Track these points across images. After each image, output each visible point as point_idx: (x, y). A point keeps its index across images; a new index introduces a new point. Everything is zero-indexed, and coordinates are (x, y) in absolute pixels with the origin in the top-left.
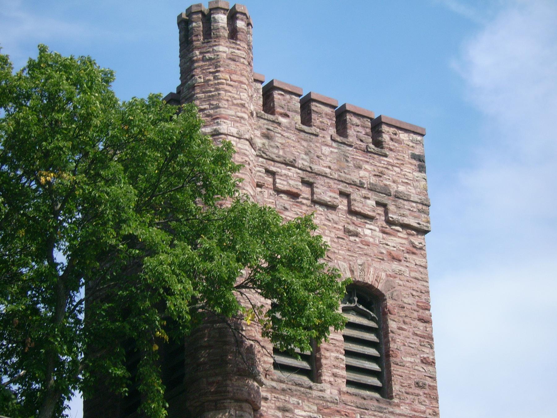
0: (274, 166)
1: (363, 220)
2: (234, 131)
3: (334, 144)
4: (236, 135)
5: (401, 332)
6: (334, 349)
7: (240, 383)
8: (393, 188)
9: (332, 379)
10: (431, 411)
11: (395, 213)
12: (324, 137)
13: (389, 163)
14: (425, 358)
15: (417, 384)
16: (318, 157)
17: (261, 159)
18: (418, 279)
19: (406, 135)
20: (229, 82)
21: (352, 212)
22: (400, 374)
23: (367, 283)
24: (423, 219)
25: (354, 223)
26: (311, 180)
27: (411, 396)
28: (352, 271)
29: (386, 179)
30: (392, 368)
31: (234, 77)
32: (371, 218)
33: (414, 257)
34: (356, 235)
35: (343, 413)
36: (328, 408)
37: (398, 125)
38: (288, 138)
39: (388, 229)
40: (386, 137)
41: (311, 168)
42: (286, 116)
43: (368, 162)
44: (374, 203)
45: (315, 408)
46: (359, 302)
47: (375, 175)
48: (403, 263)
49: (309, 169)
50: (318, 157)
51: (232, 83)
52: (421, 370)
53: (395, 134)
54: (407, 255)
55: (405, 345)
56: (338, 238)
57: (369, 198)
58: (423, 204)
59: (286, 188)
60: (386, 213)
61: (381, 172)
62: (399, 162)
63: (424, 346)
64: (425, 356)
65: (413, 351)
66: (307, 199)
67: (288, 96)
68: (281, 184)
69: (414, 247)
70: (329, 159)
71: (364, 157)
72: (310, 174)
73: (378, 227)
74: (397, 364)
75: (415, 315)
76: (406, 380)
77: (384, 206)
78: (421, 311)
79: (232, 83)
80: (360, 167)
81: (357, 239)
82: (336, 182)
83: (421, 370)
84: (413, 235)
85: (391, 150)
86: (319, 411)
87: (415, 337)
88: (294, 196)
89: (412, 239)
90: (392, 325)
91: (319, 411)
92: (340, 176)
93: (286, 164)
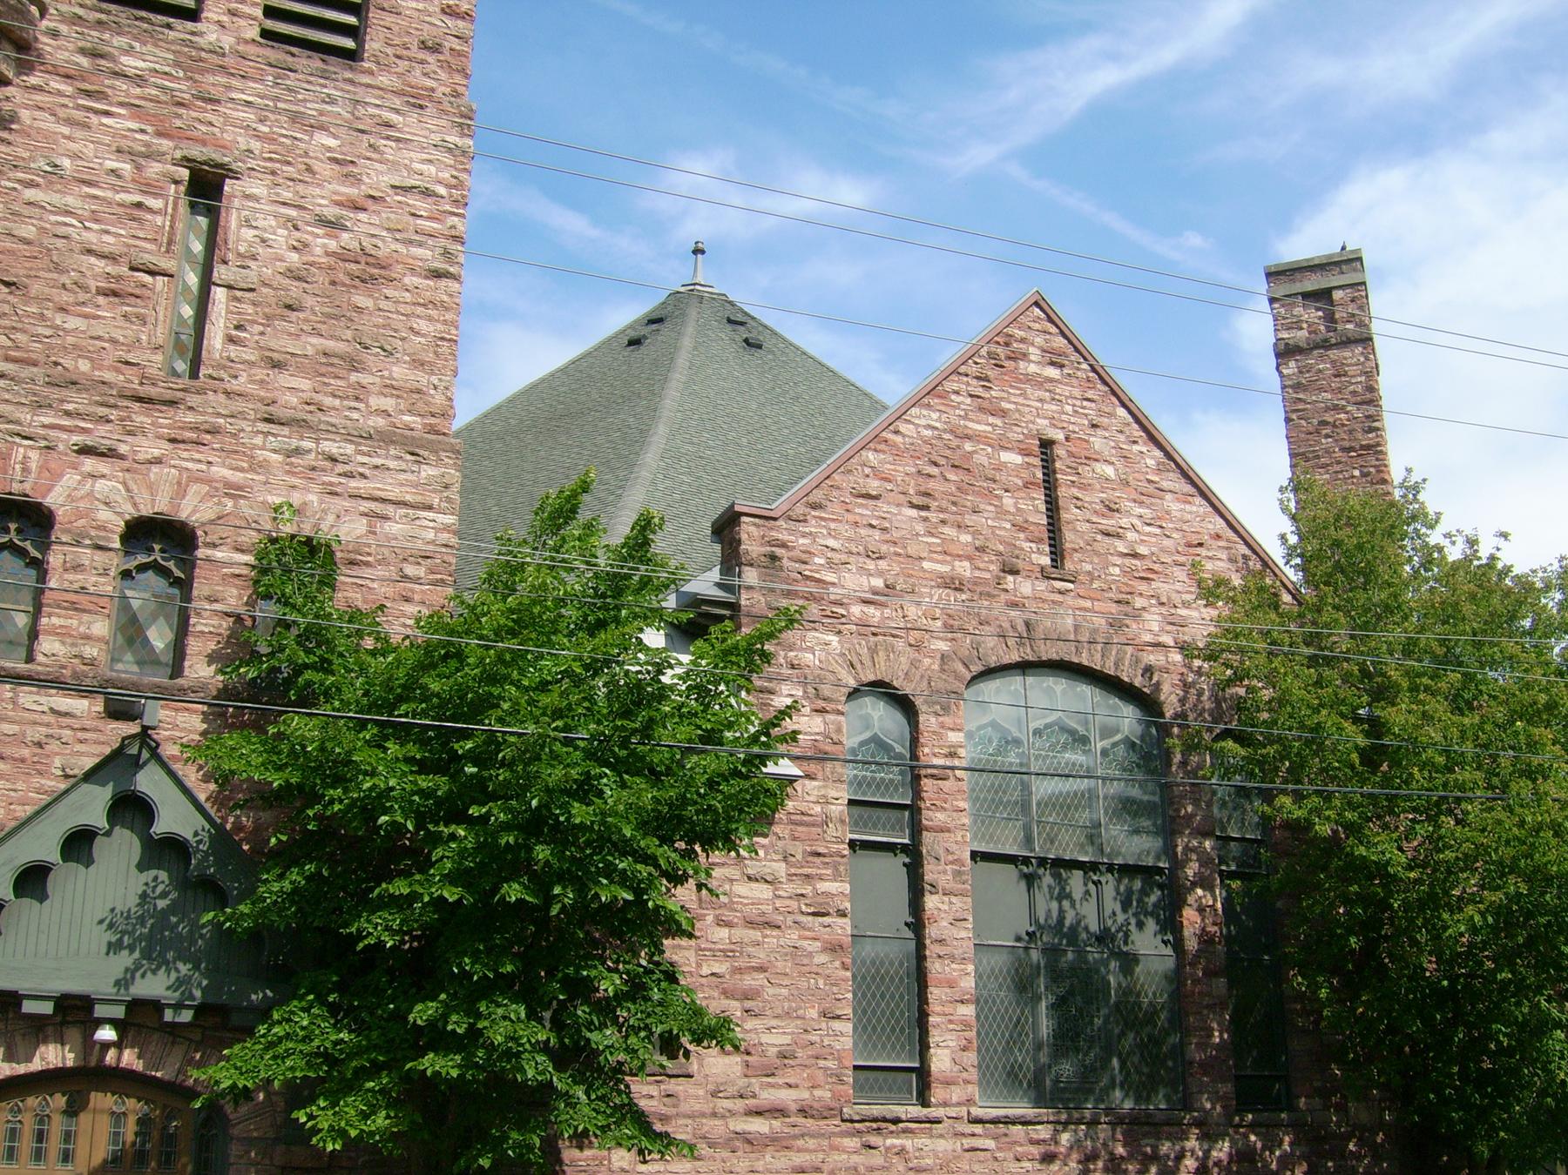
9: (225, 18)
10: (448, 90)
15: (423, 45)
74: (383, 9)
76: (399, 35)
91: (177, 64)
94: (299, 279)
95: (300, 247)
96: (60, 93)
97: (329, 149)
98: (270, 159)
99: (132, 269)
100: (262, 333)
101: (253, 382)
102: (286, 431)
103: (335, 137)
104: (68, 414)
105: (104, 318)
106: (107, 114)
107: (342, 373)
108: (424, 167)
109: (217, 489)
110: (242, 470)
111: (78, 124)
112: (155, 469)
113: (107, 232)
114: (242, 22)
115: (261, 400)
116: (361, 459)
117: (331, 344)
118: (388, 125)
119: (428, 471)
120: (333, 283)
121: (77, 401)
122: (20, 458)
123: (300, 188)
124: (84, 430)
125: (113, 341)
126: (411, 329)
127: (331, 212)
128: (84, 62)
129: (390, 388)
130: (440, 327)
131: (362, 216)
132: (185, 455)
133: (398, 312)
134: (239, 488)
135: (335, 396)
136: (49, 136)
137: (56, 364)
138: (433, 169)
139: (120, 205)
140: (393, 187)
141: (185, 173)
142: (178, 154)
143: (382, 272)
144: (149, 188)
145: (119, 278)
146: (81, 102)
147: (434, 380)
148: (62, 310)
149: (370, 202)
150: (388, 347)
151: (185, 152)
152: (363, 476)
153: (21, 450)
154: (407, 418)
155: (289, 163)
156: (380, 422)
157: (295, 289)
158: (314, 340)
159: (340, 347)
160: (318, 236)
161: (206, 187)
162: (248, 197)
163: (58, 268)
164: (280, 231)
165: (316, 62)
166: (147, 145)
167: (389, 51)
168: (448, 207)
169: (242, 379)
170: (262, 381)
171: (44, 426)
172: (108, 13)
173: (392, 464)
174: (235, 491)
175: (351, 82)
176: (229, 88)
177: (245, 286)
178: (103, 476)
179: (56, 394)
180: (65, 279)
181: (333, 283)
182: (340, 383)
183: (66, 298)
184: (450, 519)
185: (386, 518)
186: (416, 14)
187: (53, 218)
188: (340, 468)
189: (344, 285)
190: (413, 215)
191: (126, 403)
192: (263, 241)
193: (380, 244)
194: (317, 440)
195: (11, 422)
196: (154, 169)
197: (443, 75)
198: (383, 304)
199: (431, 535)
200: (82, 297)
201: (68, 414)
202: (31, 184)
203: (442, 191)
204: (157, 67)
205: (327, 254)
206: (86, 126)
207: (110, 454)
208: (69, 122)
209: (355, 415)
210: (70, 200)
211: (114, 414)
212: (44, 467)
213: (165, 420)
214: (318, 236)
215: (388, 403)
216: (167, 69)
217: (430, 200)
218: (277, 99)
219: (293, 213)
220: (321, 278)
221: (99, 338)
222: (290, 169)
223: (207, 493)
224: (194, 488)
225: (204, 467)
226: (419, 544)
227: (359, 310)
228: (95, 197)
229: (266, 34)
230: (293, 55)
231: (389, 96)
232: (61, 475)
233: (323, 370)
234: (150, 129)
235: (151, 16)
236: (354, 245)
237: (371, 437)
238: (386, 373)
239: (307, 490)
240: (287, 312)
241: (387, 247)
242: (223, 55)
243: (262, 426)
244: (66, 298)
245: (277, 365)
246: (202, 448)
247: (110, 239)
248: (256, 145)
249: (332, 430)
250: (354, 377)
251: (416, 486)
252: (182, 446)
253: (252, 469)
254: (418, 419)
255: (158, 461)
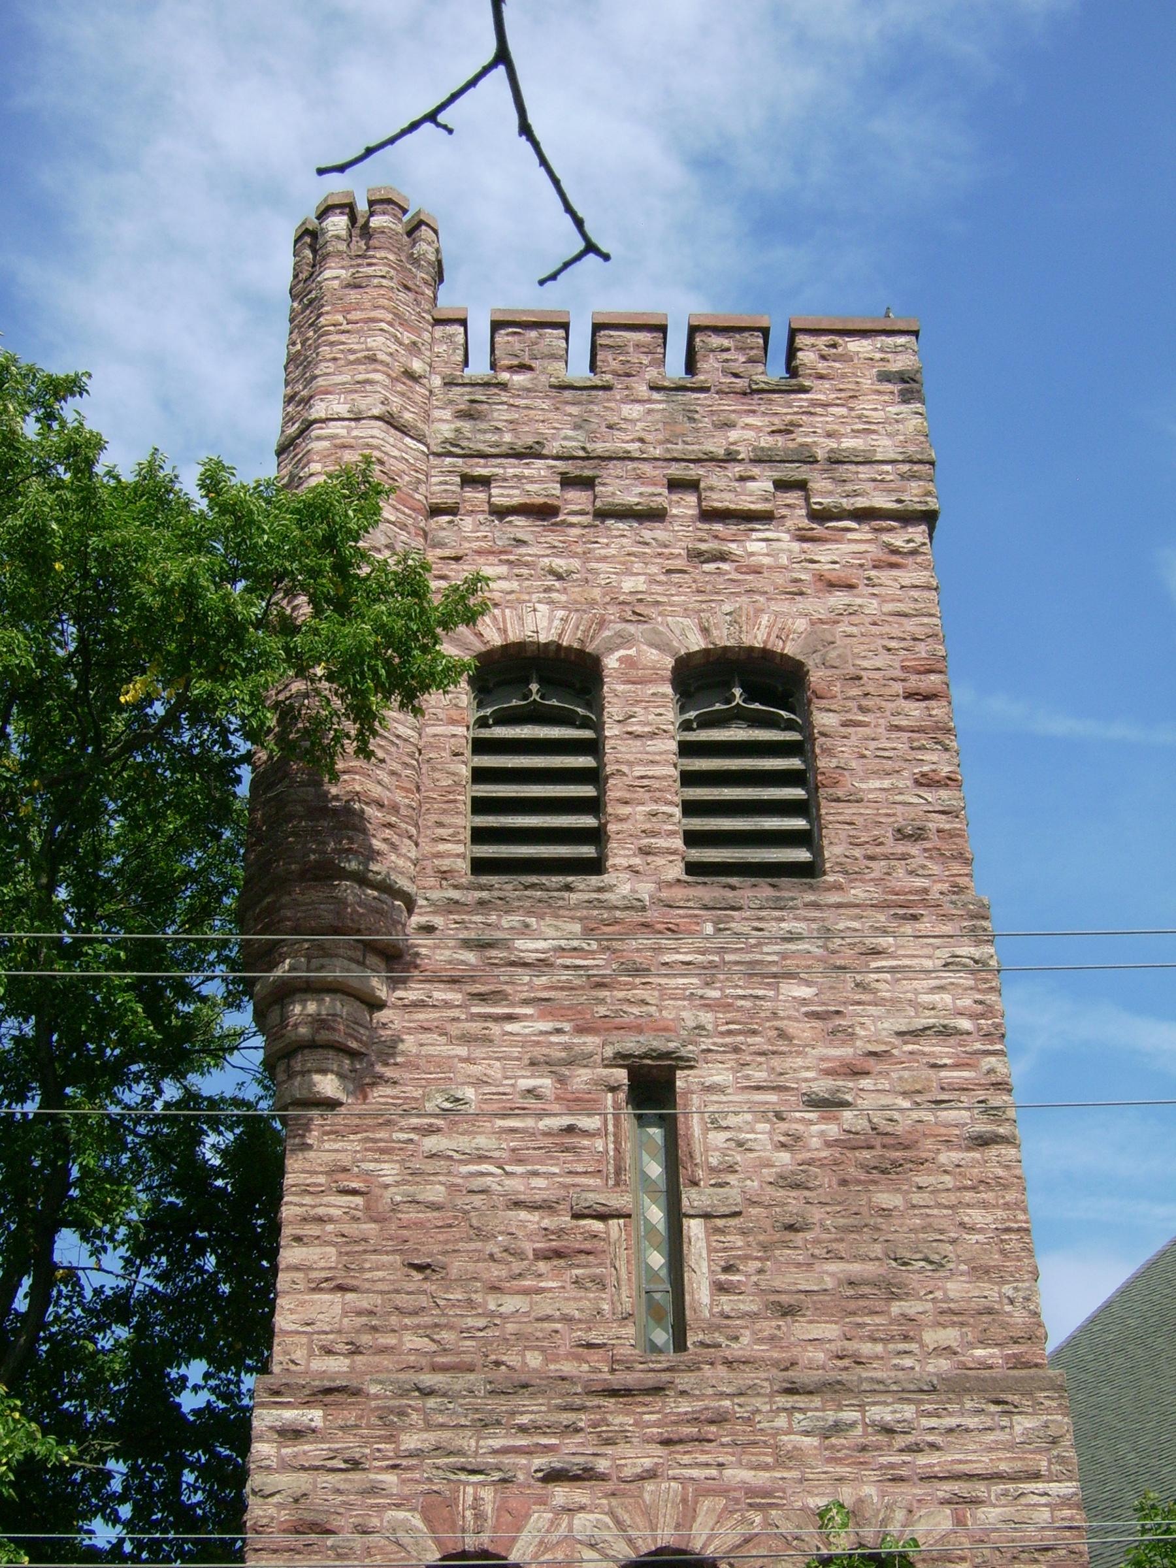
0: (485, 466)
1: (742, 527)
2: (342, 409)
3: (656, 396)
4: (348, 416)
5: (850, 730)
6: (647, 796)
7: (314, 895)
8: (823, 447)
9: (637, 861)
10: (945, 887)
11: (824, 494)
12: (627, 388)
13: (814, 403)
14: (924, 775)
15: (901, 835)
16: (610, 427)
17: (448, 460)
18: (906, 615)
19: (865, 342)
20: (345, 327)
21: (709, 515)
22: (848, 819)
23: (751, 649)
24: (915, 492)
25: (716, 537)
26: (587, 473)
27: (883, 863)
28: (705, 631)
29: (807, 435)
30: (823, 812)
31: (354, 316)
32: (766, 517)
33: (895, 573)
34: (722, 557)
35: (660, 927)
36: (616, 922)
37: (839, 326)
38: (528, 408)
39: (818, 530)
40: (806, 357)
41: (584, 449)
42: (524, 368)
43: (754, 412)
44: (770, 486)
45: (577, 928)
46: (750, 697)
47: (773, 432)
48: (863, 589)
49: (581, 453)
50: (610, 427)
51: (349, 327)
52: (916, 800)
53: (834, 346)
54: (873, 573)
55: (864, 757)
56: (669, 572)
57: (752, 478)
58: (911, 462)
59: (515, 501)
60: (807, 499)
61: (792, 424)
62: (842, 395)
63: (922, 748)
64: (925, 769)
65: (888, 765)
66: (582, 513)
67: (533, 334)
68: (502, 496)
69: (895, 551)
70: (640, 425)
71: (743, 404)
72: (586, 463)
73: (788, 531)
74: (838, 800)
75: (898, 688)
76: (866, 828)
77: (802, 486)
78: (914, 677)
79: (349, 327)
80: (730, 425)
81: (725, 566)
82: (659, 463)
83: (916, 800)
84: (890, 530)
85: (821, 377)
86: (588, 932)
87: (894, 735)
88: (543, 512)
89: (886, 537)
90: (823, 720)
91: (588, 932)
92: (668, 450)
93: (519, 456)
94: (797, 1186)
95: (791, 1143)
96: (447, 1005)
97: (804, 1002)
98: (730, 1033)
99: (576, 1216)
100: (761, 1271)
101: (760, 1341)
102: (817, 1401)
103: (809, 984)
104: (523, 1429)
105: (550, 1289)
106: (510, 1018)
107: (879, 1305)
108: (937, 997)
109: (737, 1501)
110: (766, 1467)
111: (476, 1040)
112: (649, 1486)
113: (535, 1174)
114: (660, 861)
115: (776, 1364)
116: (926, 1422)
117: (856, 1268)
118: (876, 952)
119: (1023, 1424)
120: (844, 1182)
121: (532, 1410)
122: (470, 1500)
123: (775, 1062)
124: (548, 1449)
125: (567, 1319)
126: (962, 1225)
127: (823, 1087)
128: (471, 957)
129: (950, 1315)
130: (1000, 1213)
131: (865, 1083)
132: (686, 1459)
133: (940, 1206)
134: (767, 1494)
135: (874, 1340)
136: (443, 1064)
137: (498, 1364)
138: (947, 998)
139: (546, 1134)
140: (900, 1034)
141: (621, 1075)
142: (609, 1052)
143: (908, 1154)
144: (580, 1103)
145: (560, 1232)
146: (474, 1010)
147: (1007, 1289)
148: (495, 1289)
149: (872, 1061)
150: (935, 1257)
151: (618, 1047)
152: (933, 1446)
153: (470, 1490)
154: (979, 1352)
155: (754, 1032)
156: (944, 1364)
157: (794, 1201)
158: (833, 1267)
159: (869, 1269)
160: (811, 1122)
161: (652, 1087)
162: (709, 1089)
163: (480, 1234)
164: (760, 1127)
165: (764, 890)
166: (567, 1047)
167: (858, 852)
168: (978, 1046)
169: (745, 1341)
170: (772, 1338)
171: (495, 1452)
172: (490, 888)
173: (972, 1422)
174: (761, 1499)
175: (815, 905)
176: (658, 950)
177: (727, 1210)
178: (582, 1508)
179: (501, 1405)
180: (491, 1247)
181: (844, 1182)
182: (878, 1320)
183: (497, 1272)
184: (1068, 1488)
185: (976, 1502)
186: (882, 796)
187: (464, 1169)
188: (900, 1441)
189: (859, 1182)
190: (934, 1066)
191: (597, 1401)
192: (740, 1144)
193: (896, 1115)
194: (861, 1407)
195: (450, 1454)
196: (582, 1077)
197: (935, 868)
198: (916, 1198)
199: (1045, 1515)
200: (517, 1266)
201: (523, 1429)
202: (431, 1131)
203: (965, 1024)
204: (563, 943)
205: (828, 1144)
206: (487, 1040)
207: (587, 1475)
208: (466, 1039)
209: (907, 1362)
210: (482, 1141)
211: (583, 1420)
212: (502, 1508)
213: (651, 1416)
214: (811, 1122)
215: (949, 1336)
216: (575, 943)
217: (952, 1041)
218: (722, 951)
219: (772, 1097)
220: (825, 1180)
221: (548, 1318)
222: (758, 1039)
223: (725, 1508)
224: (706, 1503)
225: (714, 1472)
226: (1031, 1531)
227: (886, 1213)
228: (513, 1130)
229: (693, 868)
230: (733, 888)
231: (869, 912)
232: (528, 1516)
233: (852, 1305)
234: (567, 1027)
235: (544, 879)
236: (862, 1124)
237: (934, 1389)
238: (939, 1294)
239: (858, 1480)
240: (790, 1236)
241: (908, 1117)
242: (644, 909)
243: (783, 1401)
244: (497, 1272)
245: (788, 1311)
246: (708, 1446)
247: (540, 1182)
248: (706, 1018)
249: (880, 1389)
250: (896, 1308)
251: (1011, 1447)
252: (679, 1448)
253: (779, 1464)
254: (996, 1351)
255: (651, 1475)
